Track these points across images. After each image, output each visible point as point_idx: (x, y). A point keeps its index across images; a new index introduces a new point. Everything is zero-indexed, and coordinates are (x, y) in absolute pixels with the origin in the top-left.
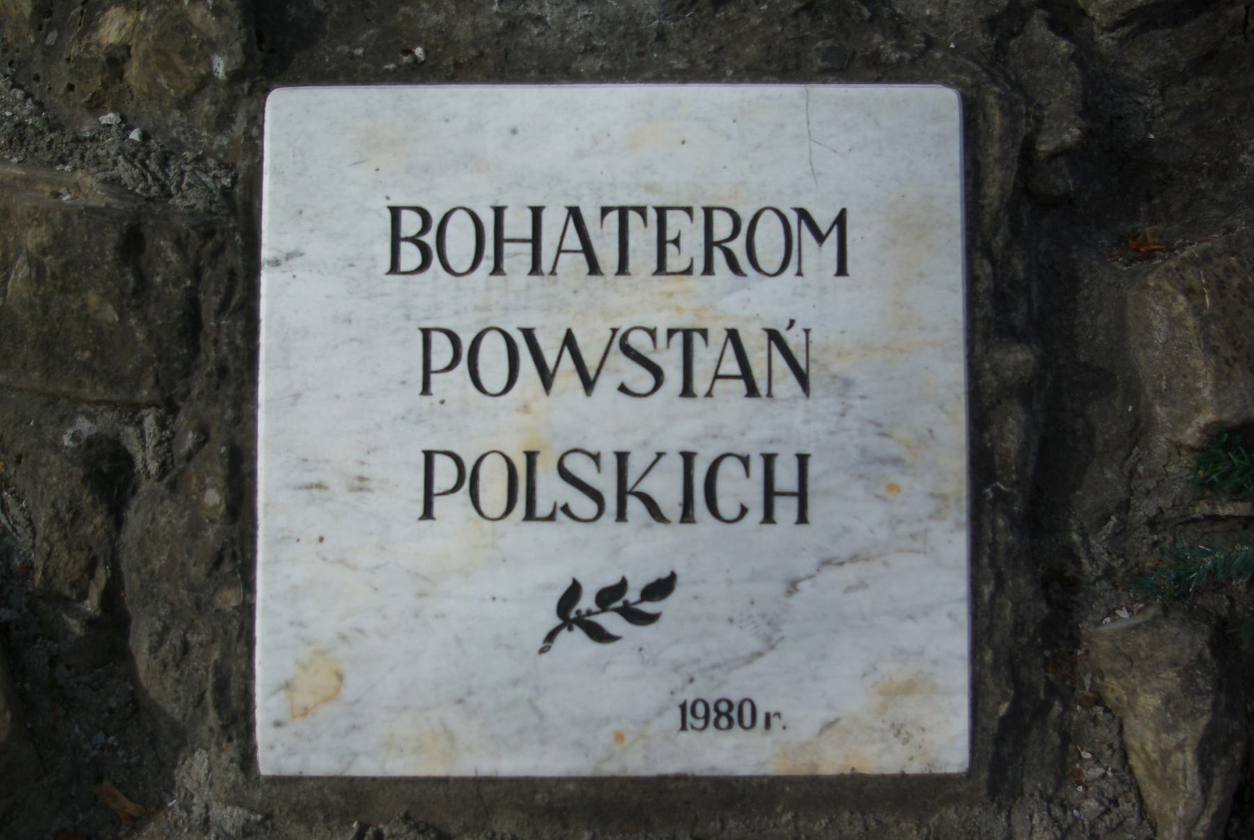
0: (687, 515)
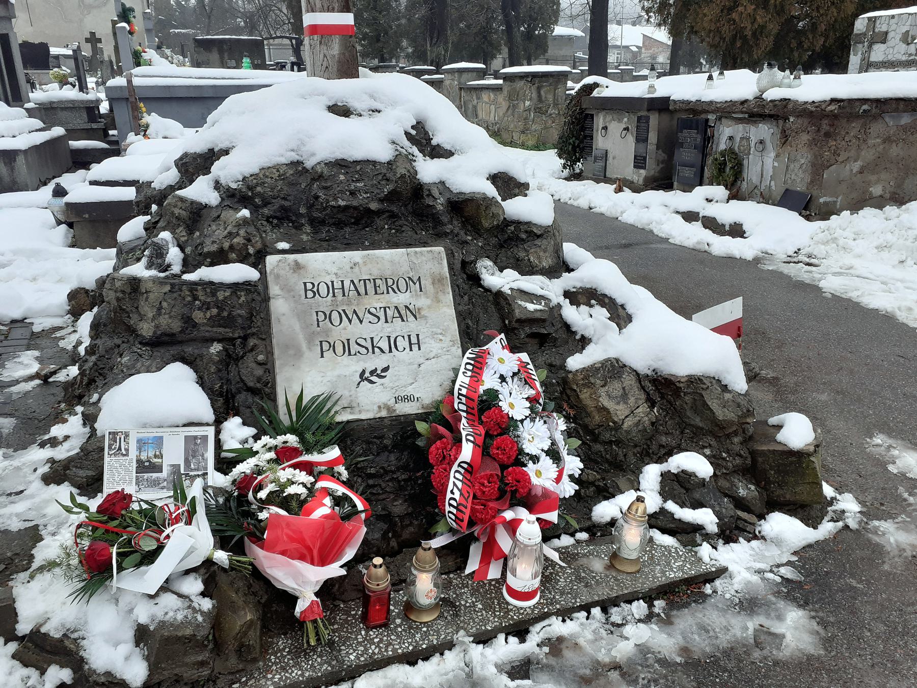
0: (390, 351)
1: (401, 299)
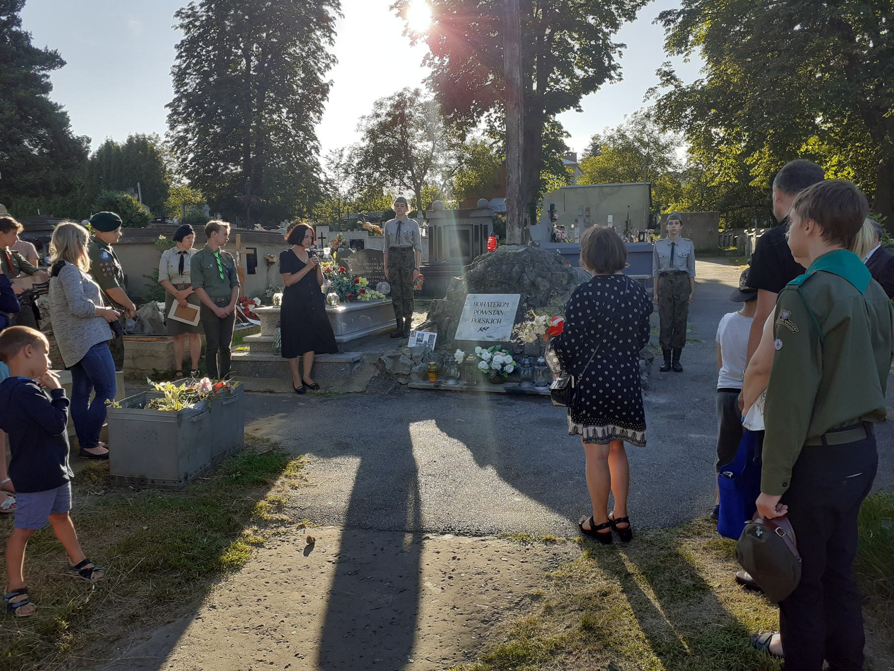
1: (499, 309)
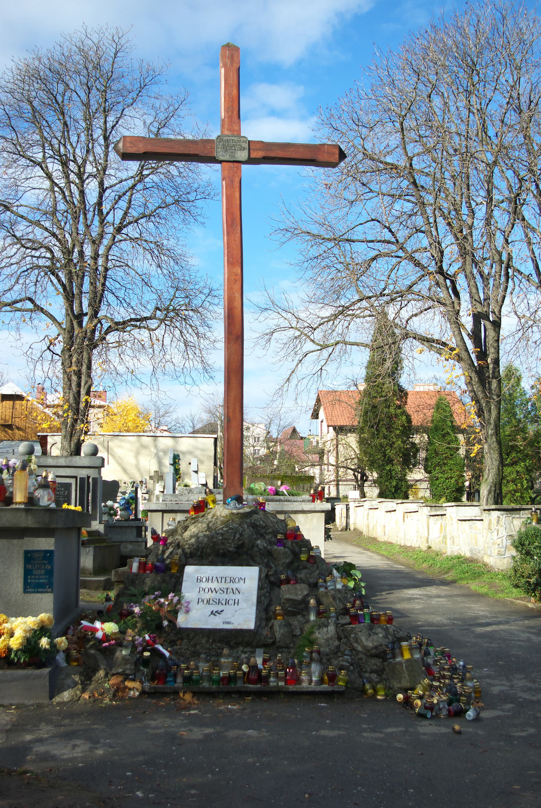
1: (234, 586)
